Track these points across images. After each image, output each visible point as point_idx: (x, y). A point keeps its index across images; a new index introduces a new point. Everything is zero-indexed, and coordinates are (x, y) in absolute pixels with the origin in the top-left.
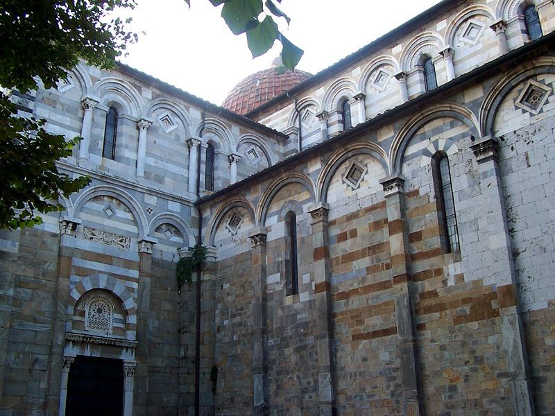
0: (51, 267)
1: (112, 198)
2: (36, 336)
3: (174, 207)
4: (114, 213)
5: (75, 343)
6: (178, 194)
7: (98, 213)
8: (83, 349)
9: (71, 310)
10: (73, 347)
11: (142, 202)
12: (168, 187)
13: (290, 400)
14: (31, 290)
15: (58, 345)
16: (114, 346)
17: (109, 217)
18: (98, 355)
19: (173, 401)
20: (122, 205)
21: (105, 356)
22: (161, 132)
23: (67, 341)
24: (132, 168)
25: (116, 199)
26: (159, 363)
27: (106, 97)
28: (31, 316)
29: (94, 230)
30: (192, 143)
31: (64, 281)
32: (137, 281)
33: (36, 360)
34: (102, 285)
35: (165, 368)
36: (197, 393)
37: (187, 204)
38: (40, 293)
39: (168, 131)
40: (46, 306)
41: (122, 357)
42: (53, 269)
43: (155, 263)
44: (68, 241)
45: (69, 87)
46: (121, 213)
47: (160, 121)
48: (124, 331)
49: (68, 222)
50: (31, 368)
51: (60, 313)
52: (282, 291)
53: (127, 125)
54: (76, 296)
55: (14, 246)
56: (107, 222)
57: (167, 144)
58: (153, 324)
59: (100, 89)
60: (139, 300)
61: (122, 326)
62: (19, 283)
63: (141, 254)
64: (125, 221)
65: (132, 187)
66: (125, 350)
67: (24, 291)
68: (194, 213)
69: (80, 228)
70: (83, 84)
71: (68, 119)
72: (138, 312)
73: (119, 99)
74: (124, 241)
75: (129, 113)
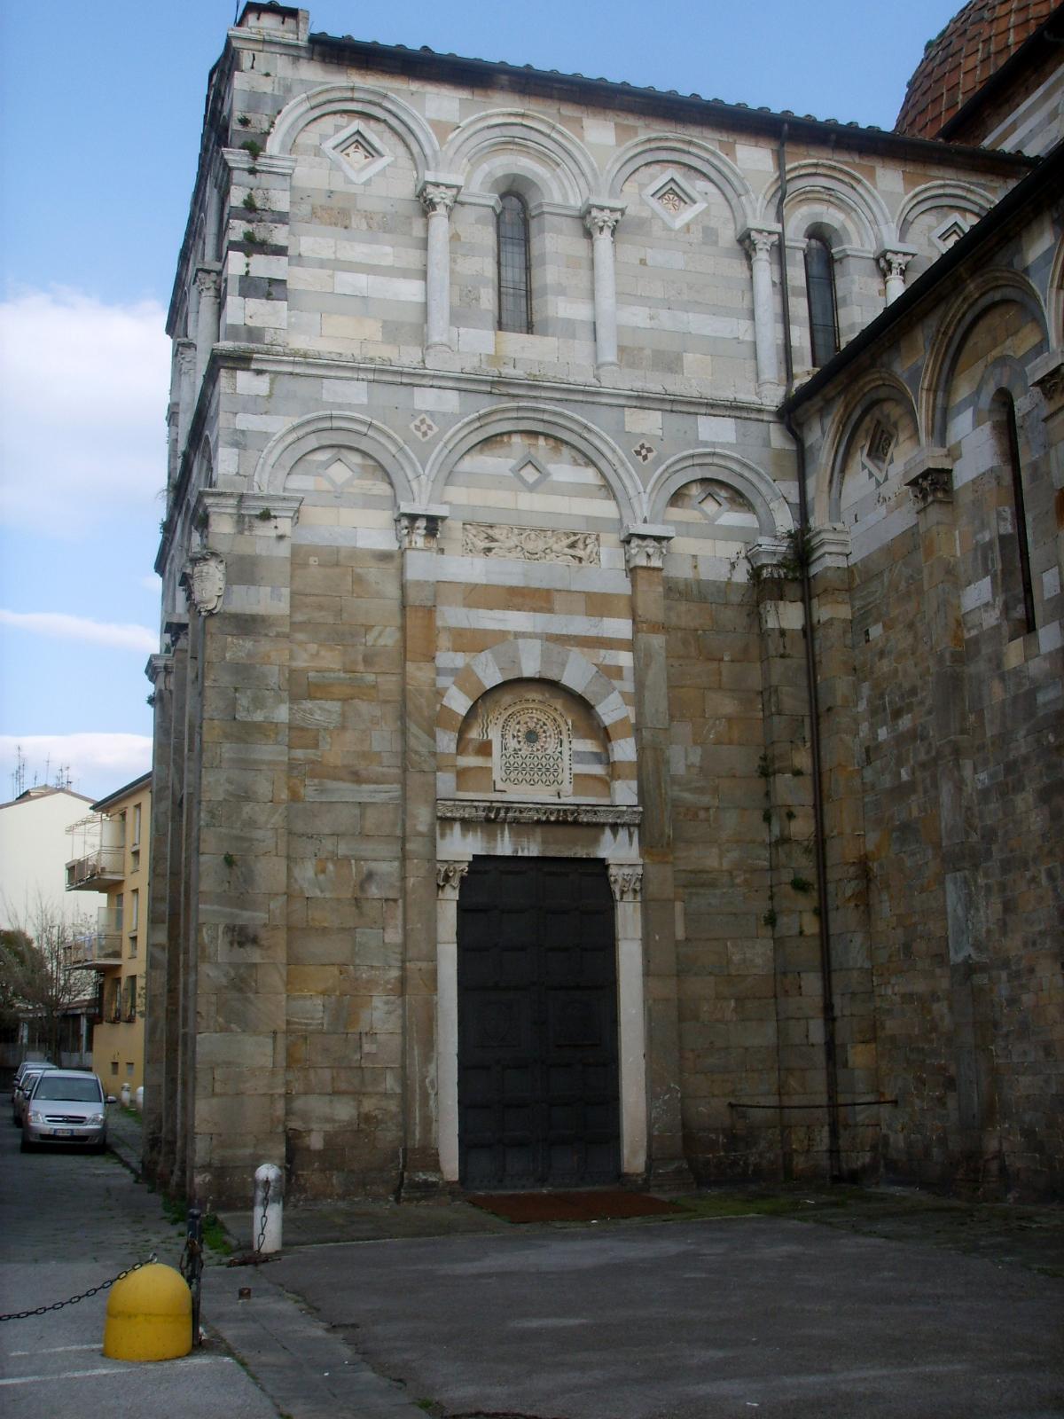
1: (534, 434)
2: (362, 816)
3: (718, 431)
5: (467, 824)
6: (727, 394)
7: (497, 482)
8: (491, 837)
9: (446, 741)
10: (464, 836)
11: (620, 431)
12: (695, 378)
13: (1034, 944)
14: (339, 704)
15: (420, 834)
16: (576, 823)
17: (532, 488)
19: (759, 961)
20: (565, 450)
21: (552, 852)
22: (657, 230)
23: (446, 821)
24: (582, 347)
25: (547, 436)
26: (711, 859)
27: (485, 167)
28: (345, 766)
29: (491, 527)
30: (753, 244)
31: (420, 669)
32: (630, 645)
33: (370, 876)
34: (530, 669)
35: (730, 873)
36: (825, 936)
37: (753, 415)
38: (363, 707)
39: (678, 223)
40: (383, 740)
41: (601, 854)
43: (673, 590)
44: (422, 565)
45: (380, 164)
46: (564, 471)
47: (653, 202)
48: (605, 783)
49: (413, 518)
50: (359, 894)
51: (416, 752)
52: (998, 627)
54: (459, 703)
57: (677, 260)
58: (682, 758)
59: (465, 149)
60: (637, 699)
61: (598, 770)
62: (302, 688)
63: (632, 571)
64: (579, 490)
65: (588, 396)
66: (608, 832)
67: (320, 708)
68: (777, 437)
69: (454, 526)
70: (415, 148)
71: (388, 249)
72: (637, 730)
73: (524, 164)
74: (581, 545)
75: (557, 198)
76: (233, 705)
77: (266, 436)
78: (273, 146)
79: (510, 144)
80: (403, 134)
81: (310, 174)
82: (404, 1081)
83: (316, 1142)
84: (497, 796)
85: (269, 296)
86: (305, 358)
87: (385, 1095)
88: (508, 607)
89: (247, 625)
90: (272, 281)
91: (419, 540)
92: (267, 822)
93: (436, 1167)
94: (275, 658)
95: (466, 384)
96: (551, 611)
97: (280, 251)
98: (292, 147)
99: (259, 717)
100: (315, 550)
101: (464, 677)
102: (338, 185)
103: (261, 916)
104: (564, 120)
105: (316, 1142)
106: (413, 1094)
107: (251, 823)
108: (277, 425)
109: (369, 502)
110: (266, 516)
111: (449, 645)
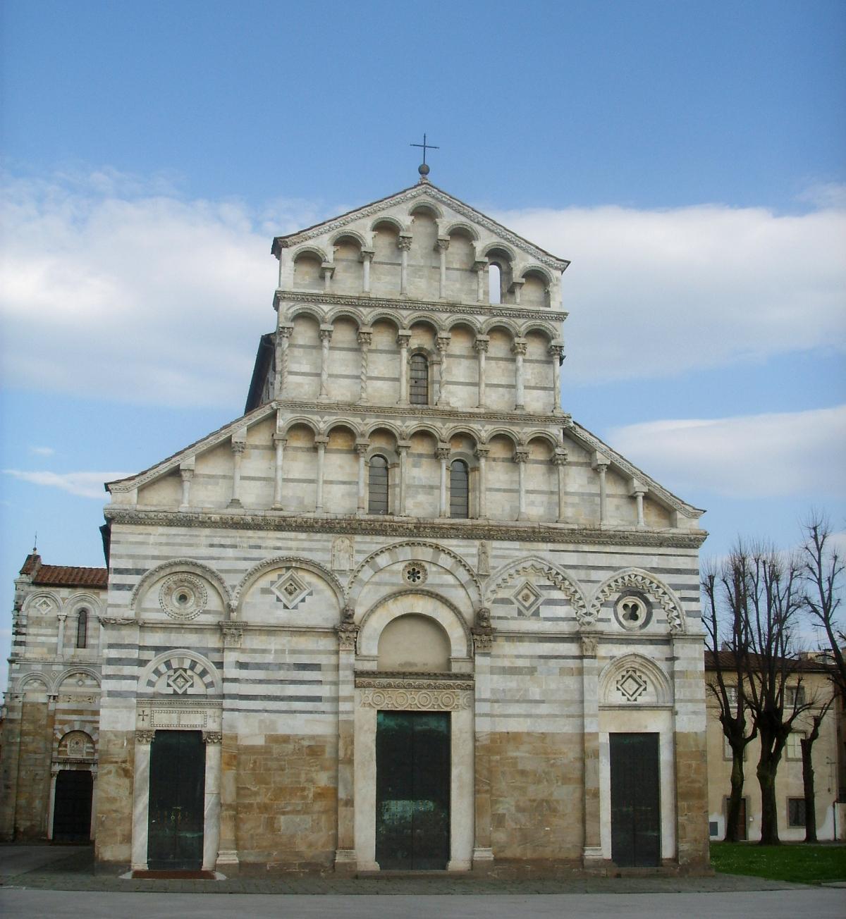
0: (44, 722)
4: (84, 682)
7: (71, 685)
9: (56, 745)
17: (80, 686)
18: (75, 769)
27: (76, 606)
33: (37, 774)
34: (76, 729)
40: (41, 745)
44: (52, 706)
46: (89, 682)
48: (94, 753)
53: (91, 621)
54: (59, 736)
55: (18, 715)
56: (79, 690)
61: (92, 751)
62: (22, 734)
64: (92, 686)
65: (94, 665)
73: (85, 605)
76: (8, 738)
77: (18, 678)
78: (23, 608)
79: (82, 600)
80: (55, 601)
81: (32, 613)
83: (22, 830)
84: (68, 757)
85: (21, 645)
86: (27, 660)
87: (38, 821)
88: (72, 714)
89: (12, 721)
90: (21, 642)
91: (52, 701)
92: (14, 763)
93: (46, 834)
94: (17, 729)
95: (64, 664)
96: (83, 715)
97: (24, 634)
98: (28, 607)
99: (13, 741)
100: (28, 703)
101: (61, 731)
102: (39, 615)
103: (11, 783)
104: (94, 593)
105: (22, 830)
107: (11, 763)
108: (21, 676)
109: (42, 691)
110: (17, 697)
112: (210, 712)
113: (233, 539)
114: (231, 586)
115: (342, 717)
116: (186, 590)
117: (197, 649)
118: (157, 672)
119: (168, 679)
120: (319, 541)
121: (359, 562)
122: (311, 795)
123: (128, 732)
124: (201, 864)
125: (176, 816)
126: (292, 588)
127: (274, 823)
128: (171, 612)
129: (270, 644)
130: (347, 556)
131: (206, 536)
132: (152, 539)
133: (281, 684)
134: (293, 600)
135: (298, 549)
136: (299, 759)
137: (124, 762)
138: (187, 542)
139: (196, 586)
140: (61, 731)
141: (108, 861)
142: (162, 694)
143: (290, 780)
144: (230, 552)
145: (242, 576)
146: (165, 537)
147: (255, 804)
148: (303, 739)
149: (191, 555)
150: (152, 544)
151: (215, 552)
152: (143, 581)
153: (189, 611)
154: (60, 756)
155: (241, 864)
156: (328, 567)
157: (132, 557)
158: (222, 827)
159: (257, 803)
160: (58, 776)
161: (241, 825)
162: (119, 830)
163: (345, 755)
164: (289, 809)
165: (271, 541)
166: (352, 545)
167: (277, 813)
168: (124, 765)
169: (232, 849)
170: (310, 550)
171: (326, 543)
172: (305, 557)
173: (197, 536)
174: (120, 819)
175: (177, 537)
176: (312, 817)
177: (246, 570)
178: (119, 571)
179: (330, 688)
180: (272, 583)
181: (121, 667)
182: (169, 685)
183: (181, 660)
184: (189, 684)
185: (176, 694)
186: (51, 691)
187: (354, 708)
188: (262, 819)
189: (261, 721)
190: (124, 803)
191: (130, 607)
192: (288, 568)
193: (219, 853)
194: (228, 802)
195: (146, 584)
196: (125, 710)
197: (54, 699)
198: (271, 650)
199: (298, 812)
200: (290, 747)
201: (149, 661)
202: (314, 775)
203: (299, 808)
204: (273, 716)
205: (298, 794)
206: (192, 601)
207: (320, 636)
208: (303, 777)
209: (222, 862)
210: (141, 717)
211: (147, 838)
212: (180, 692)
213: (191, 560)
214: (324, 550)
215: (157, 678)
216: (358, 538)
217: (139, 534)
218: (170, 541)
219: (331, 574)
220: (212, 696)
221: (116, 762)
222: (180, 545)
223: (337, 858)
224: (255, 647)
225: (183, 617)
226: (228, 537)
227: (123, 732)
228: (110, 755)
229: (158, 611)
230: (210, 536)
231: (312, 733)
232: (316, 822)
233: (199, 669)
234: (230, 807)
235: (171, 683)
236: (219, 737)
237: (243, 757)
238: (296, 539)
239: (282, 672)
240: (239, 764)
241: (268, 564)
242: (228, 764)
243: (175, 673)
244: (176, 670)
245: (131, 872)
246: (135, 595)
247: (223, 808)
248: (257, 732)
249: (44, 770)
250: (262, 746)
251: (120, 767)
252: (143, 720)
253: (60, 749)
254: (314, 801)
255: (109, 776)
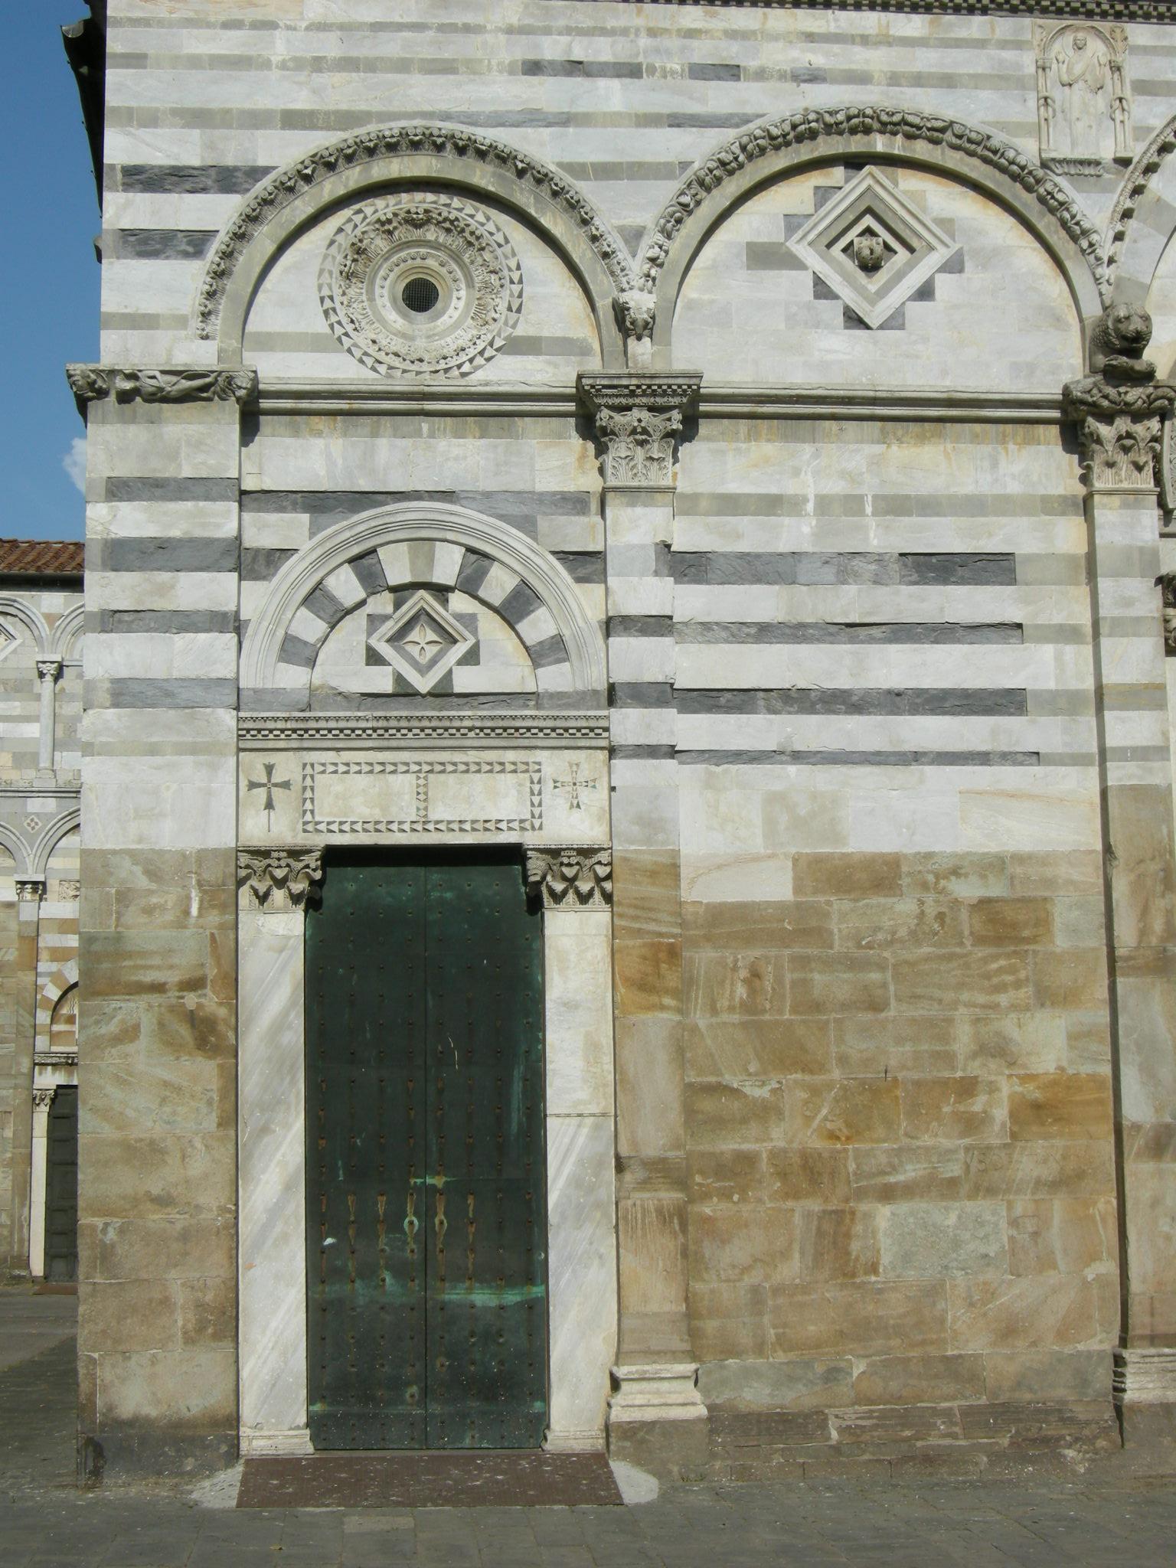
8: (71, 1074)
9: (43, 1017)
10: (53, 1073)
15: (23, 1074)
42: (12, 958)
44: (28, 910)
49: (23, 883)
54: (54, 993)
69: (53, 885)
70: (36, 633)
82: (12, 1217)
91: (28, 896)
93: (27, 1265)
101: (56, 977)
106: (21, 1225)
111: (48, 958)
112: (553, 763)
113: (622, 43)
114: (621, 230)
115: (1119, 774)
116: (434, 264)
117: (486, 500)
118: (316, 598)
119: (370, 634)
120: (981, 44)
121: (1150, 130)
122: (1001, 1113)
123: (203, 856)
124: (540, 1423)
125: (426, 1214)
126: (876, 244)
127: (848, 1235)
128: (372, 350)
129: (796, 472)
130: (1100, 102)
131: (510, 31)
132: (280, 47)
133: (852, 640)
134: (883, 292)
135: (894, 79)
136: (950, 957)
137: (195, 984)
138: (428, 53)
139: (474, 242)
140: (56, 977)
141: (133, 1422)
142: (346, 696)
143: (908, 1048)
144: (612, 94)
145: (665, 193)
146: (333, 37)
147: (764, 1165)
148: (955, 872)
149: (443, 107)
150: (283, 66)
151: (549, 93)
152: (252, 218)
153: (450, 343)
154: (54, 1049)
155: (718, 1420)
156: (1027, 151)
157: (198, 118)
158: (627, 1259)
159: (774, 1154)
160: (53, 1100)
161: (708, 1249)
162: (178, 1285)
163: (1143, 933)
164: (910, 1172)
165: (780, 44)
166: (1119, 59)
167: (860, 1194)
168: (191, 1000)
169: (674, 1356)
170: (948, 81)
171: (1008, 55)
172: (927, 111)
173: (467, 29)
174: (185, 1236)
175: (384, 36)
176: (1010, 1206)
177: (684, 165)
178: (143, 179)
179: (1058, 658)
180: (792, 222)
181: (165, 576)
182: (374, 658)
183: (423, 544)
184: (460, 649)
185: (404, 692)
186: (25, 872)
187: (1165, 735)
188: (797, 1219)
189: (774, 799)
190: (198, 1166)
191: (196, 323)
192: (854, 162)
193: (621, 1372)
194: (651, 1151)
195: (264, 239)
196: (190, 759)
197: (35, 891)
198: (805, 500)
199: (949, 1188)
200: (905, 906)
201: (286, 553)
202: (1008, 1025)
203: (954, 1170)
204: (824, 778)
205: (946, 1109)
206: (455, 304)
207: (1003, 441)
208: (963, 1038)
209: (636, 1415)
210: (262, 793)
211: (302, 1316)
212: (423, 684)
213: (448, 127)
214: (1004, 81)
215: (322, 626)
216: (1140, 33)
217: (227, 25)
218: (354, 54)
219: (1038, 181)
220: (559, 698)
221: (158, 988)
222: (403, 66)
223: (1130, 1382)
224: (733, 487)
225: (425, 367)
226: (603, 32)
227: (183, 855)
228: (130, 955)
229: (315, 344)
230: (524, 30)
231: (992, 847)
232: (1030, 1226)
233: (499, 584)
234: (660, 1170)
235: (385, 650)
236: (602, 871)
237: (703, 958)
238: (886, 40)
239: (851, 590)
240: (690, 982)
241: (777, 142)
242: (643, 986)
243: (397, 606)
244: (401, 592)
245: (242, 1461)
246: (219, 275)
247: (628, 1177)
248: (757, 844)
249: (16, 1087)
250: (781, 906)
251: (177, 1010)
252: (269, 805)
253: (56, 1028)
254: (1014, 1136)
255: (130, 1048)
